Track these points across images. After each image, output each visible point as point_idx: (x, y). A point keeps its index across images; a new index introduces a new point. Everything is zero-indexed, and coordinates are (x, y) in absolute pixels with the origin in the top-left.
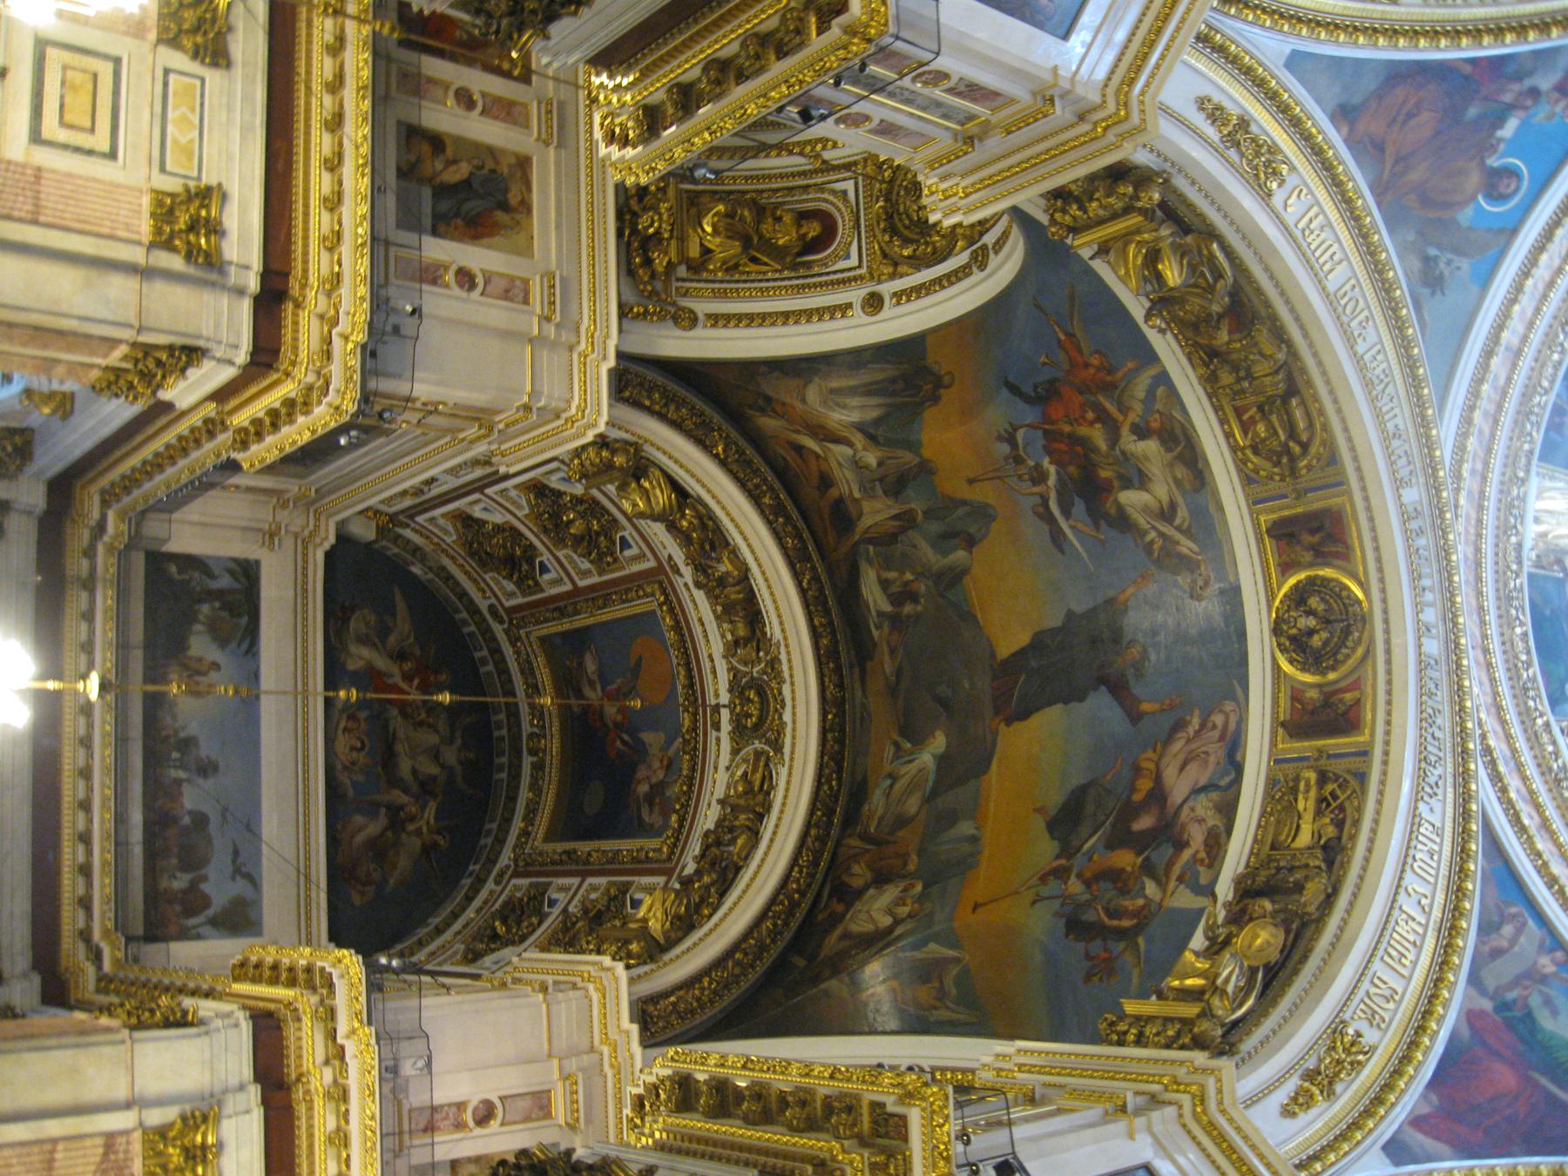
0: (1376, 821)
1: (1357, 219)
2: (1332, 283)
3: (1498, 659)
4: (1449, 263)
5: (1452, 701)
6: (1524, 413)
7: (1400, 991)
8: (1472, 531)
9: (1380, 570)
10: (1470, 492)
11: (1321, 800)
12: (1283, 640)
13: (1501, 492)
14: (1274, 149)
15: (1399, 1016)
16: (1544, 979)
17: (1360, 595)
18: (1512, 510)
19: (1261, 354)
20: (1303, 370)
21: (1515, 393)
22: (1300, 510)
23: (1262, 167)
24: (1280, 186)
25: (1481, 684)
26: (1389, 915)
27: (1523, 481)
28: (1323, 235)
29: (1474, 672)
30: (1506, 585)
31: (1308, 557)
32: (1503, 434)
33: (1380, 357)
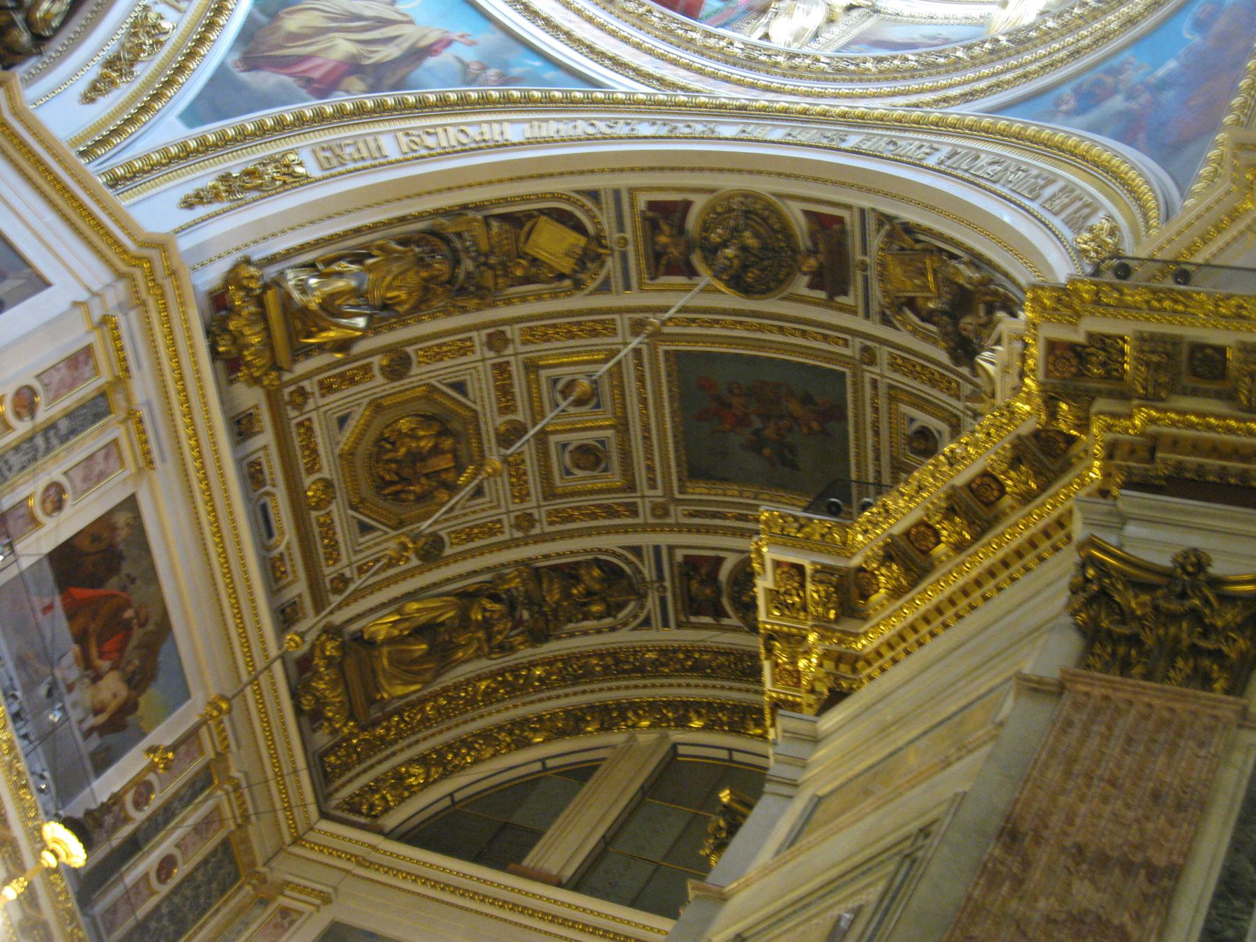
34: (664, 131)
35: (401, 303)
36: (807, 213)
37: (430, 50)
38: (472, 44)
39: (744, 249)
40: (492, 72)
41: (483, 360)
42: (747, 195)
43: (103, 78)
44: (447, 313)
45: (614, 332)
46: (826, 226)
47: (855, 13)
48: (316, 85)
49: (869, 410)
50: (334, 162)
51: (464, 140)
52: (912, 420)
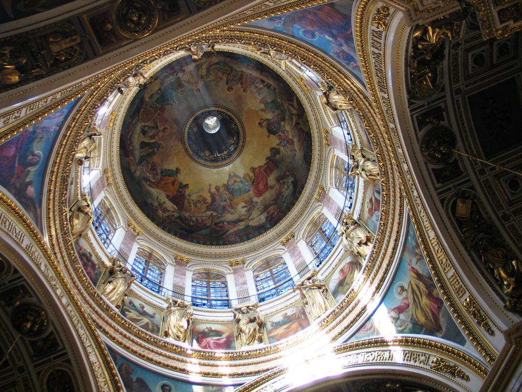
11: (72, 47)
34: (414, 187)
35: (503, 252)
36: (420, 131)
37: (417, 273)
39: (439, 145)
41: (514, 220)
42: (422, 151)
43: (459, 376)
44: (501, 237)
45: (487, 180)
46: (421, 122)
47: (364, 154)
48: (439, 305)
49: (477, 84)
50: (462, 289)
51: (440, 250)
52: (473, 67)
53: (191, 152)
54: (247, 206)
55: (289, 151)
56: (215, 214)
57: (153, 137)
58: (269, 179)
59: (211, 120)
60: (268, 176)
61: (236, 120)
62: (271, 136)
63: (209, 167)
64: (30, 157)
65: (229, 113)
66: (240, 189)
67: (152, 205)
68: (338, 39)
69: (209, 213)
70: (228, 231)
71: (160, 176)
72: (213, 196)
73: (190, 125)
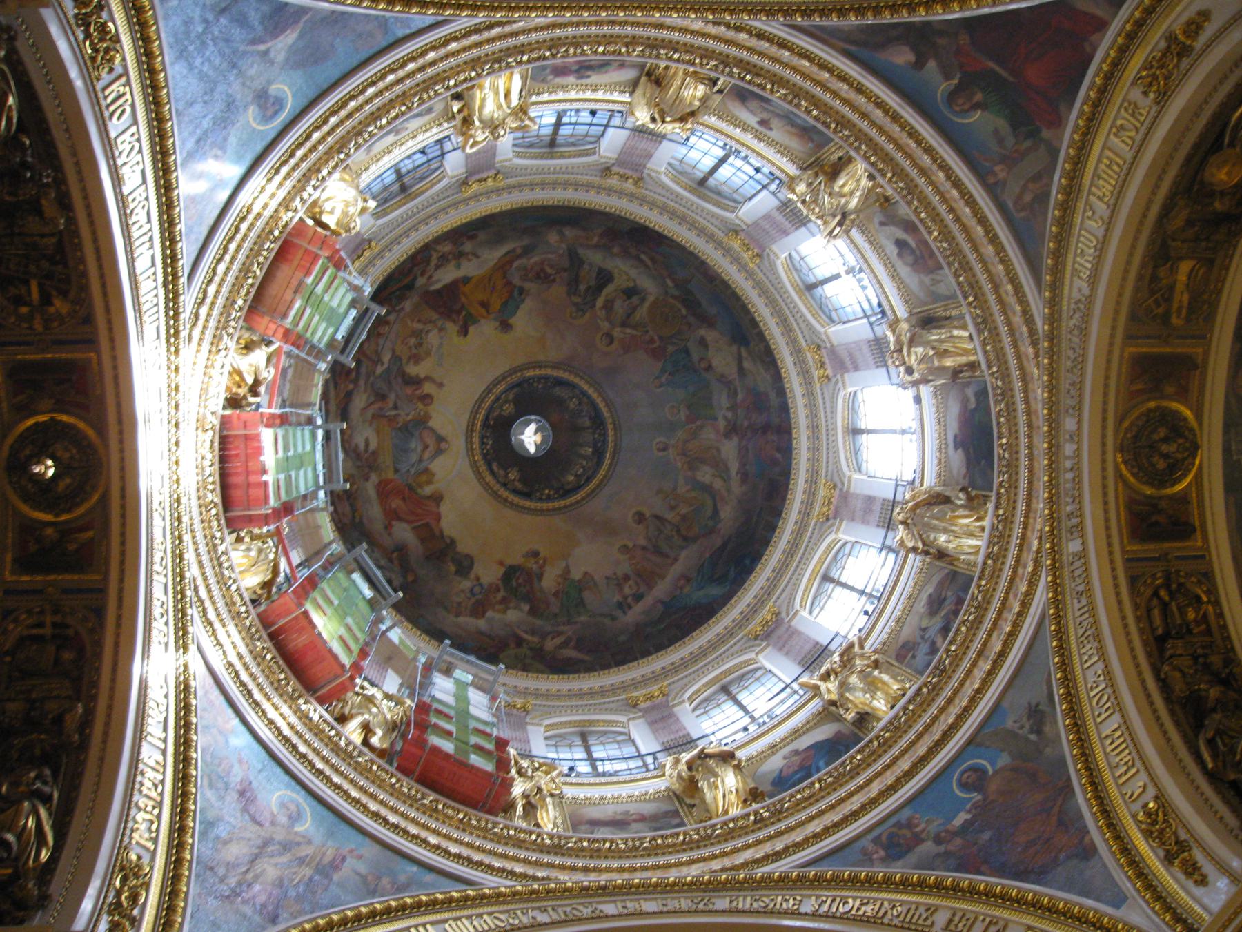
0: (1124, 279)
1: (1088, 769)
2: (1115, 721)
3: (1022, 418)
4: (1022, 727)
5: (1058, 380)
6: (982, 609)
7: (1112, 136)
8: (1031, 521)
9: (1105, 487)
10: (1029, 550)
11: (1169, 300)
12: (1191, 437)
13: (1006, 550)
14: (1148, 834)
15: (1114, 113)
16: (1004, 160)
17: (1122, 466)
18: (999, 538)
19: (1184, 674)
20: (1149, 655)
21: (987, 624)
22: (1167, 545)
23: (1159, 823)
24: (1147, 804)
25: (1036, 399)
26: (1118, 199)
27: (988, 556)
28: (1117, 759)
29: (1040, 405)
30: (1010, 477)
31: (1163, 504)
32: (1000, 594)
33: (1086, 657)
37: (335, 865)
38: (360, 857)
40: (385, 881)
53: (531, 373)
54: (366, 450)
55: (458, 600)
56: (379, 370)
57: (609, 306)
58: (405, 525)
59: (538, 438)
60: (413, 528)
61: (562, 503)
62: (502, 571)
63: (481, 400)
64: (979, 97)
65: (582, 493)
66: (406, 451)
67: (471, 238)
68: (958, 841)
69: (386, 358)
70: (336, 385)
71: (516, 281)
72: (416, 382)
73: (589, 397)
